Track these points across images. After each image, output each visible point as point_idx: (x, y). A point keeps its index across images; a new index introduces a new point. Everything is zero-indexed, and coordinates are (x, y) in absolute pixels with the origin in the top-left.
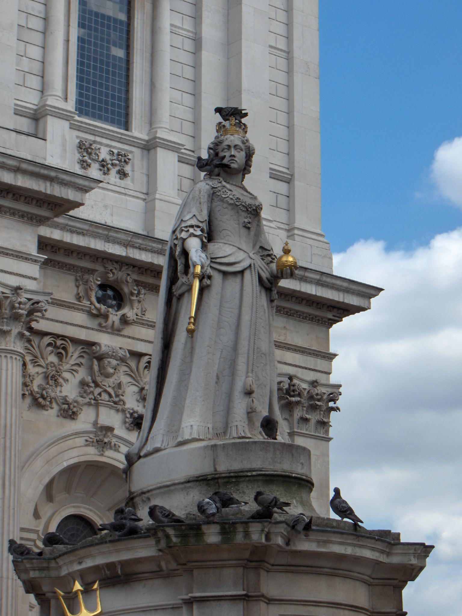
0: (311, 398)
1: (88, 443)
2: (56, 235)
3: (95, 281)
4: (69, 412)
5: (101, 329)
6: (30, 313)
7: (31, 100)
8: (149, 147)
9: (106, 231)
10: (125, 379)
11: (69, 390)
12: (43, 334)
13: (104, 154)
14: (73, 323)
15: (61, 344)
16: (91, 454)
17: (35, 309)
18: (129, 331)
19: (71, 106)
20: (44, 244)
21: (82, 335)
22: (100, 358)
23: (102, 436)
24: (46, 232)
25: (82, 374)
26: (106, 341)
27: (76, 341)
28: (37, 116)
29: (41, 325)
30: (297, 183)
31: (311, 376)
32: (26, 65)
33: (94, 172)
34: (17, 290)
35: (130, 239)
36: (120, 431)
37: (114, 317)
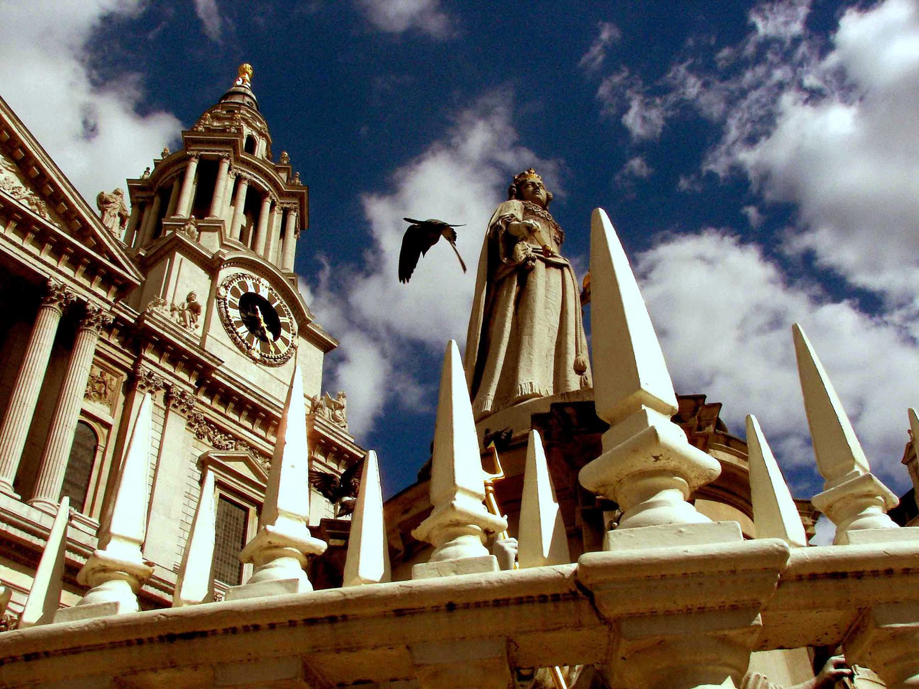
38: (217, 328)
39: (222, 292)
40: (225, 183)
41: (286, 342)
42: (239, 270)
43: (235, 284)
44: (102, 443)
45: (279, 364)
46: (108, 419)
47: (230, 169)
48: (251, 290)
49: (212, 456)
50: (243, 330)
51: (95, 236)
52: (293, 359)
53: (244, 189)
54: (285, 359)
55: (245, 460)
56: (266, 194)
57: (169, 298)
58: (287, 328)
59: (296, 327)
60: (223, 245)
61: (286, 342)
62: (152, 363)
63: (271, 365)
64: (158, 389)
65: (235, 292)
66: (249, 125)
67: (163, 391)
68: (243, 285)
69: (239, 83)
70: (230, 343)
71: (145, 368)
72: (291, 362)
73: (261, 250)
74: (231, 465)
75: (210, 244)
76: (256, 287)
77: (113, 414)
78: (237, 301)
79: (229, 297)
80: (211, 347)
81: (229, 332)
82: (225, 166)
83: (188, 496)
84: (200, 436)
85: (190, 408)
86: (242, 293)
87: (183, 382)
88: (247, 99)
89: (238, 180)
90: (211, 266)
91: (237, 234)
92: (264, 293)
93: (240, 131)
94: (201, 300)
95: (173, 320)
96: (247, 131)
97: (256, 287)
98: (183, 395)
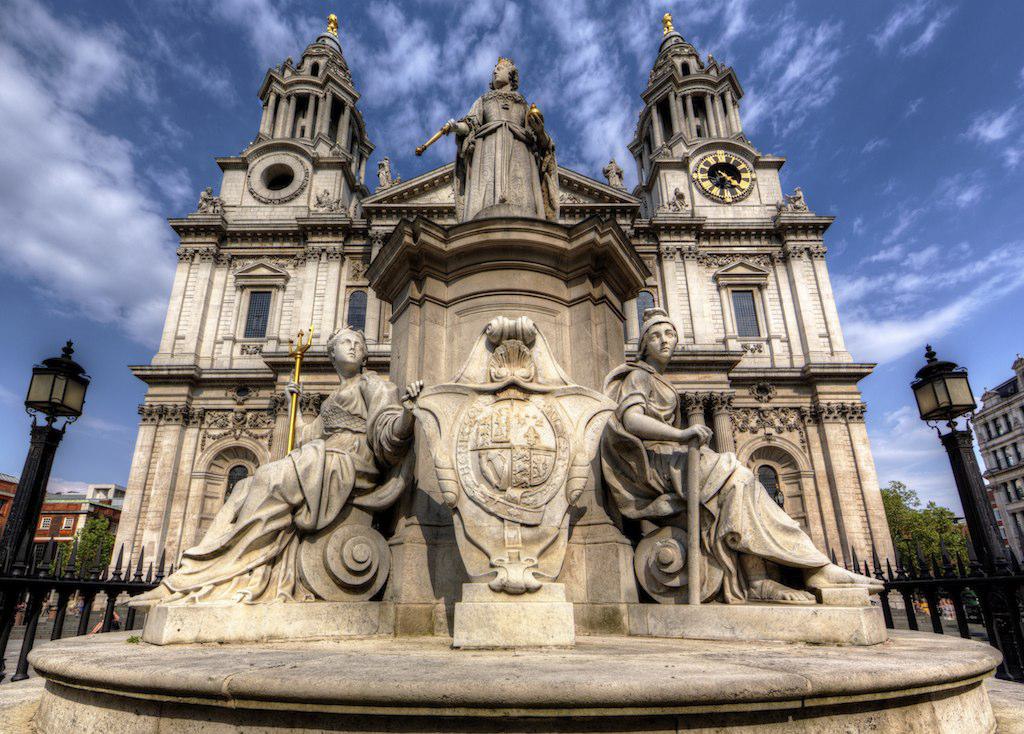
0: (853, 409)
1: (764, 440)
2: (737, 375)
3: (755, 387)
4: (754, 431)
5: (761, 402)
6: (729, 400)
7: (721, 336)
8: (768, 341)
9: (750, 370)
10: (774, 417)
11: (753, 424)
12: (738, 409)
13: (752, 346)
14: (751, 402)
15: (746, 410)
16: (766, 443)
17: (730, 399)
18: (772, 401)
19: (736, 334)
20: (729, 378)
21: (754, 405)
22: (762, 412)
23: (768, 436)
24: (731, 375)
25: (757, 418)
26: (763, 406)
27: (752, 408)
28: (725, 342)
29: (734, 405)
30: (832, 336)
31: (851, 402)
32: (717, 326)
33: (749, 353)
34: (722, 394)
35: (765, 370)
36: (774, 433)
37: (765, 398)
38: (699, 199)
39: (695, 176)
40: (676, 107)
41: (747, 180)
42: (701, 156)
43: (702, 166)
44: (655, 297)
45: (747, 197)
46: (655, 283)
47: (676, 96)
48: (713, 162)
49: (719, 272)
50: (716, 191)
51: (607, 195)
52: (755, 187)
53: (689, 102)
54: (749, 191)
55: (742, 264)
56: (705, 94)
57: (666, 200)
58: (745, 171)
59: (751, 166)
60: (688, 147)
61: (747, 180)
62: (668, 242)
63: (741, 200)
64: (674, 253)
65: (703, 171)
66: (679, 56)
67: (678, 253)
68: (706, 164)
69: (665, 33)
70: (709, 203)
71: (664, 246)
72: (755, 190)
73: (714, 134)
74: (733, 272)
75: (680, 150)
76: (716, 159)
77: (656, 280)
78: (706, 176)
79: (701, 176)
80: (700, 212)
81: (707, 197)
82: (672, 97)
83: (713, 300)
84: (709, 265)
85: (696, 254)
86: (707, 168)
87: (688, 242)
88: (674, 39)
89: (684, 98)
90: (683, 165)
91: (695, 134)
92: (722, 159)
93: (673, 66)
94: (684, 190)
95: (670, 211)
96: (678, 62)
97: (716, 159)
98: (690, 249)
